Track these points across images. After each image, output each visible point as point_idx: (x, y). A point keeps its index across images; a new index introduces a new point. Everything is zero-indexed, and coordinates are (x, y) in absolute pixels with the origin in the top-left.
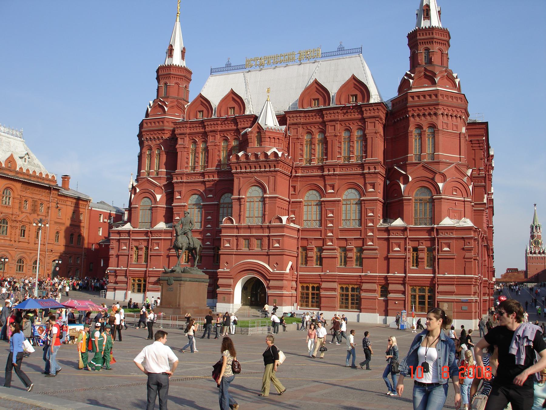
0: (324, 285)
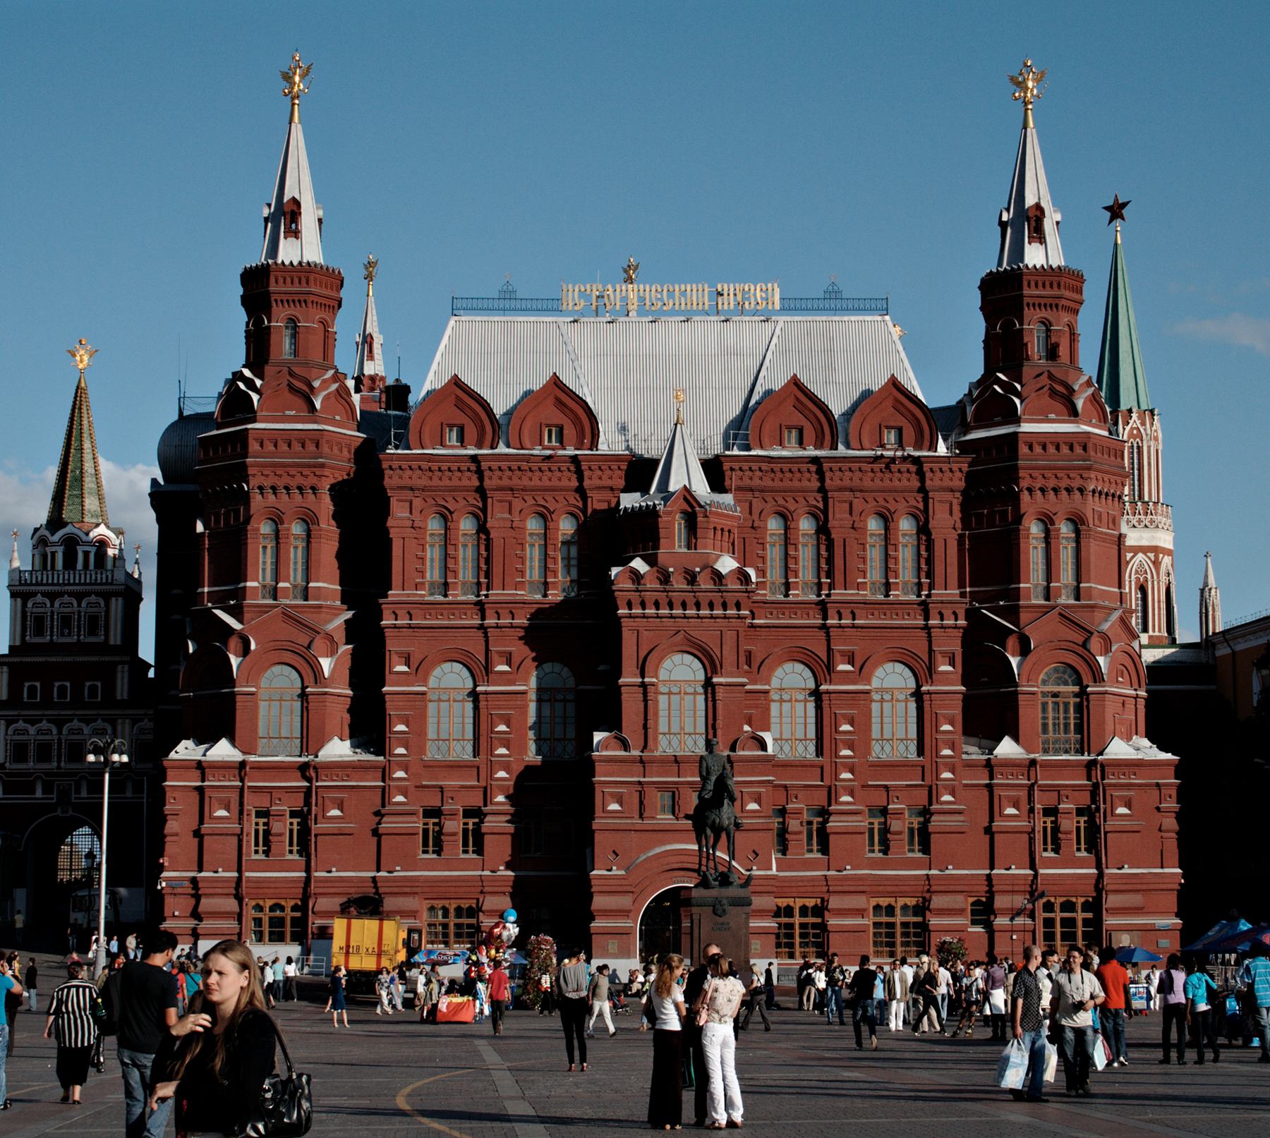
0: (834, 902)
